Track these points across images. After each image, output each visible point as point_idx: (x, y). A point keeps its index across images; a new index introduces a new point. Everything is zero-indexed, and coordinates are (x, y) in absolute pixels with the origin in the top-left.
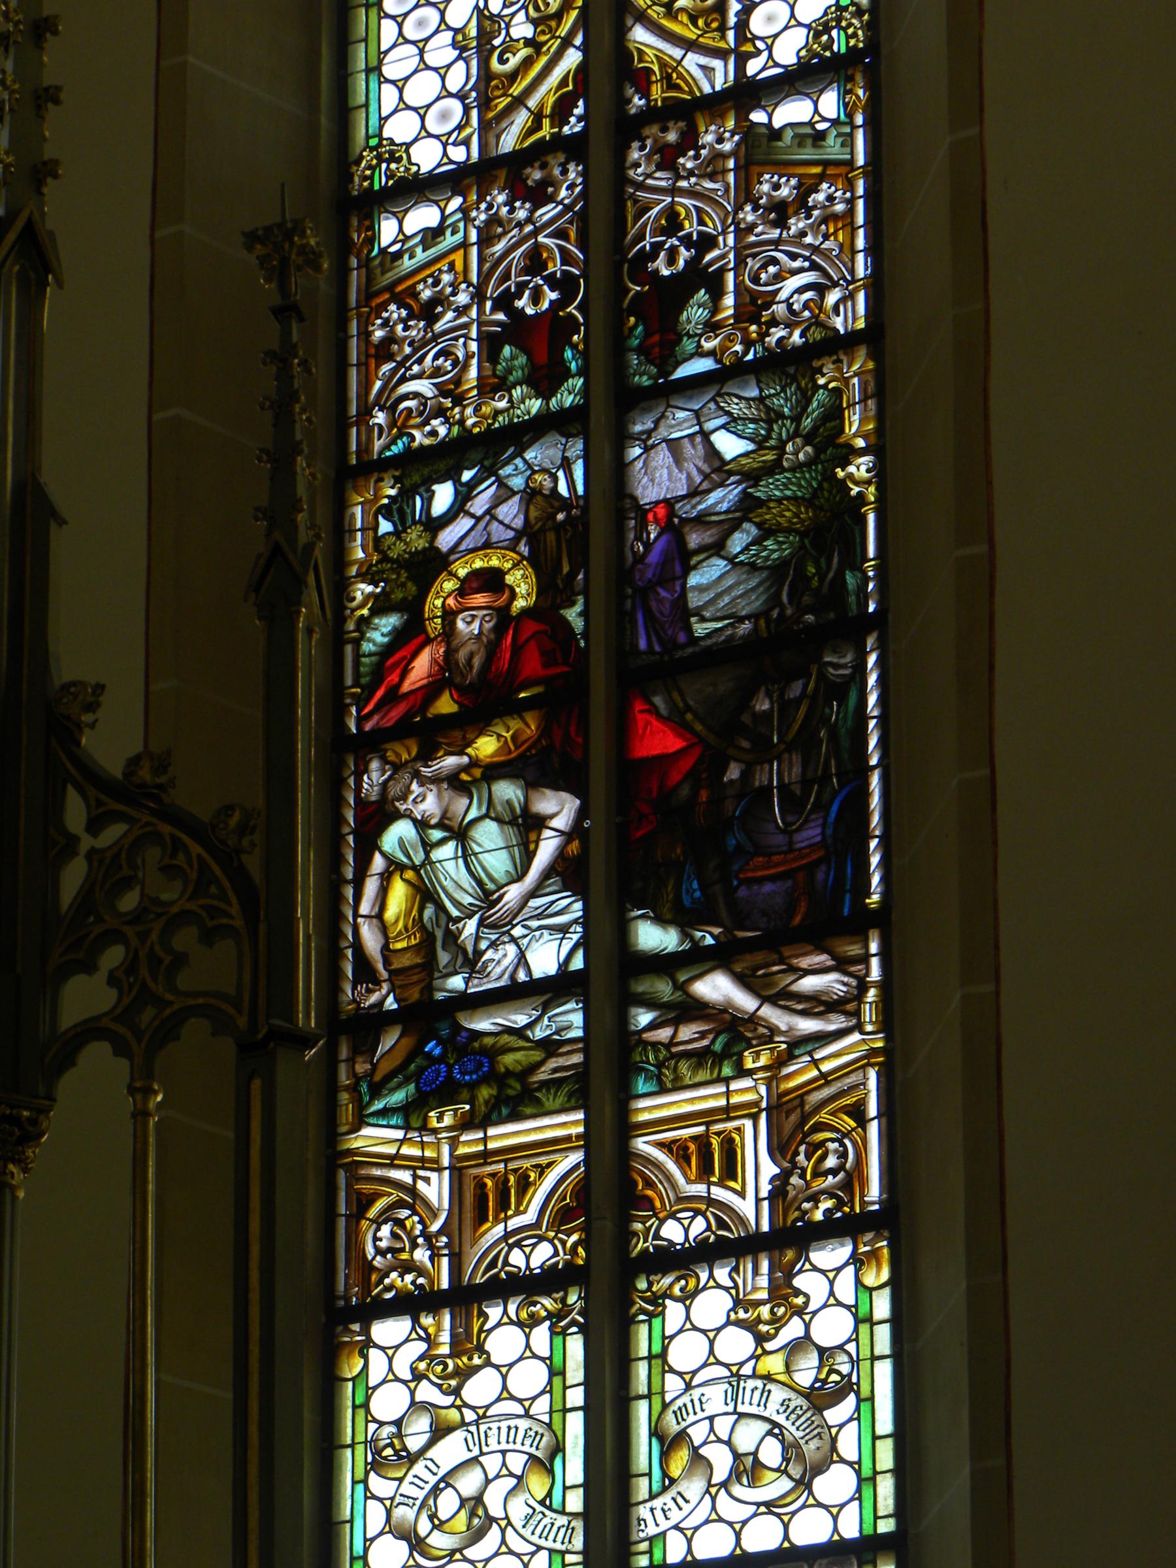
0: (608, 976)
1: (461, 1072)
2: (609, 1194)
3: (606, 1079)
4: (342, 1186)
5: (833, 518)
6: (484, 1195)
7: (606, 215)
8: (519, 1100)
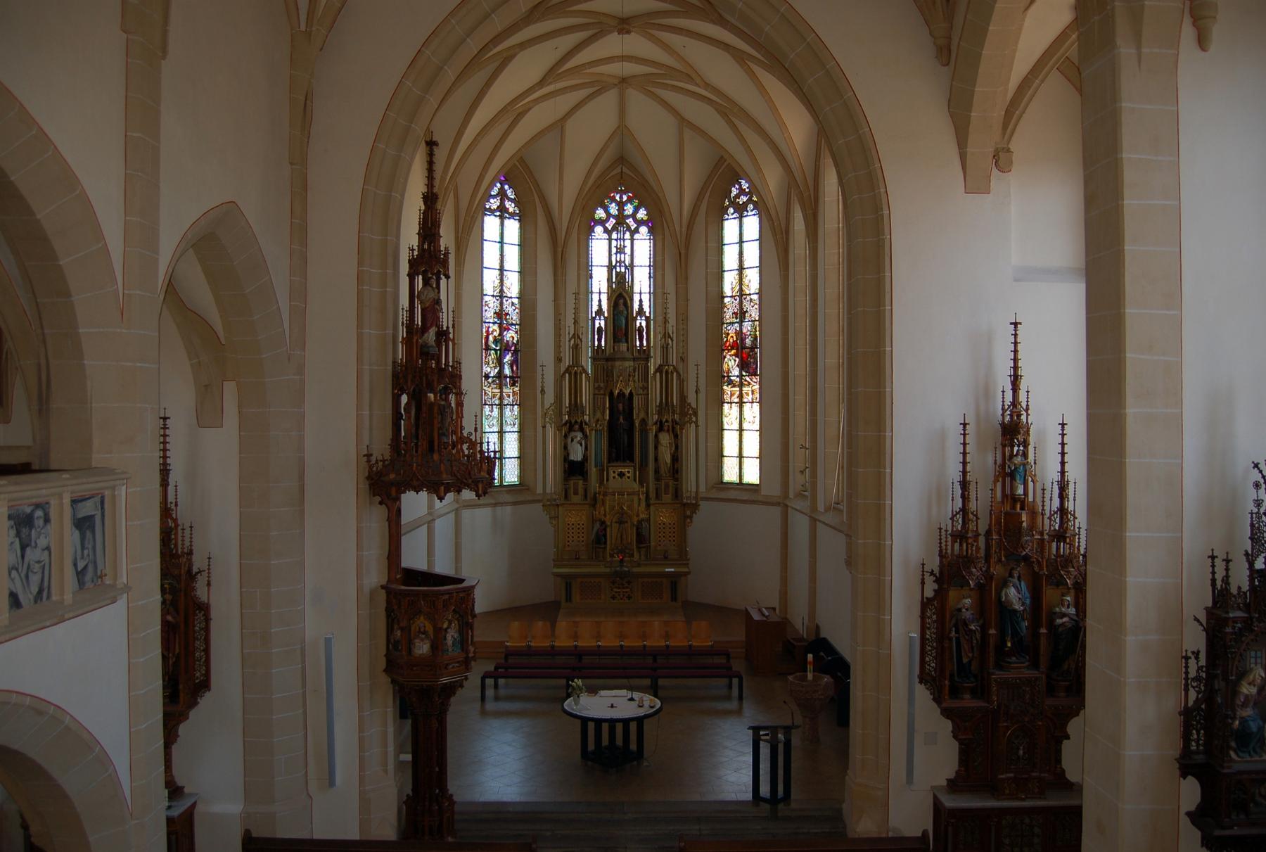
0: (741, 376)
1: (731, 383)
2: (741, 396)
3: (741, 385)
4: (722, 392)
5: (756, 338)
6: (732, 395)
7: (741, 303)
8: (734, 386)
